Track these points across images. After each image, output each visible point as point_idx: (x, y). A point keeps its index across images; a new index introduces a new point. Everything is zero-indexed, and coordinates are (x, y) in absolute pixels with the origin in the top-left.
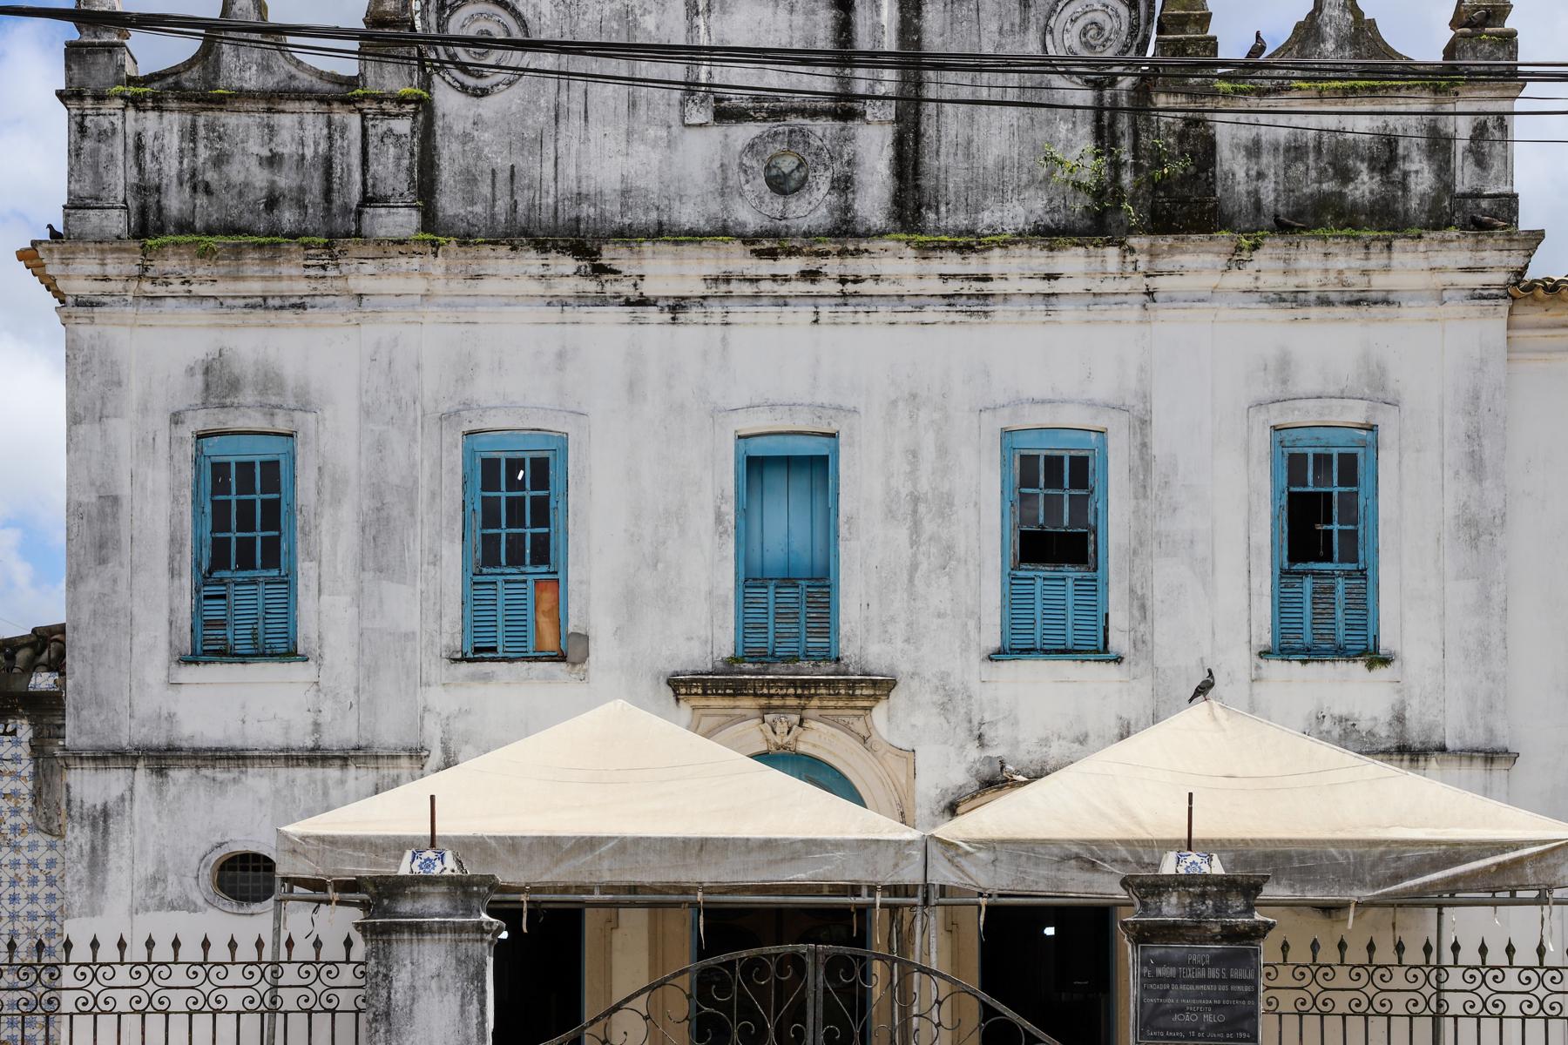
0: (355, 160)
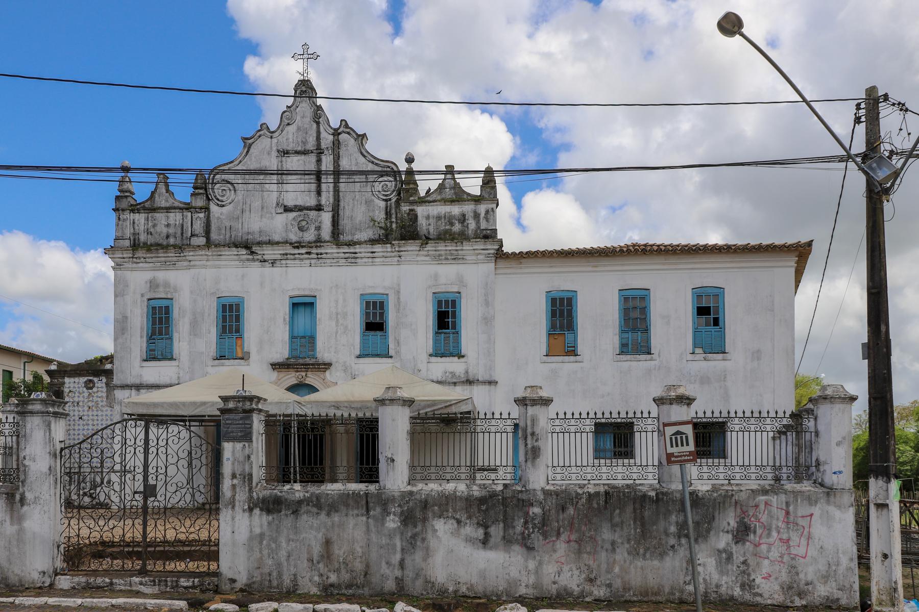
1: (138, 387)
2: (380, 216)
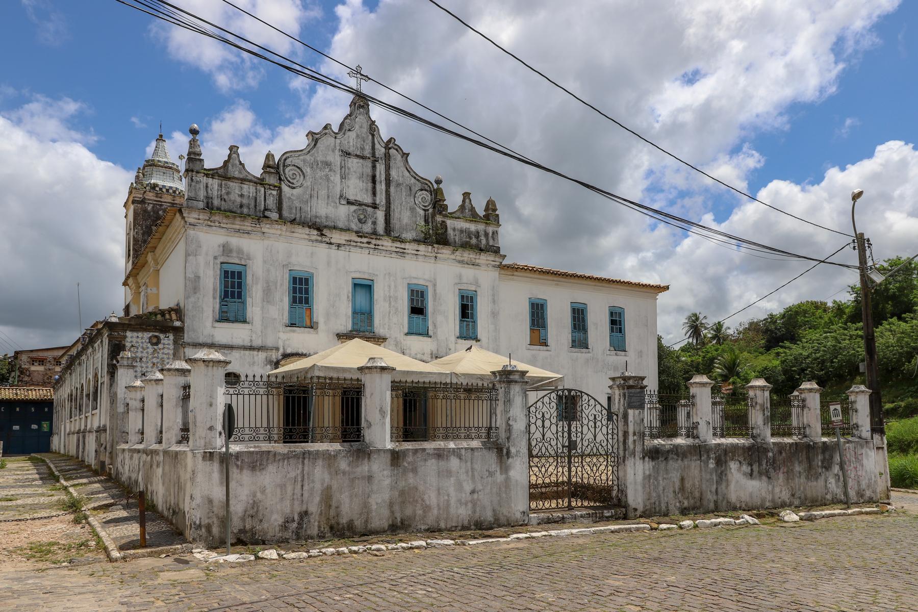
0: (263, 199)
1: (211, 346)
2: (423, 223)
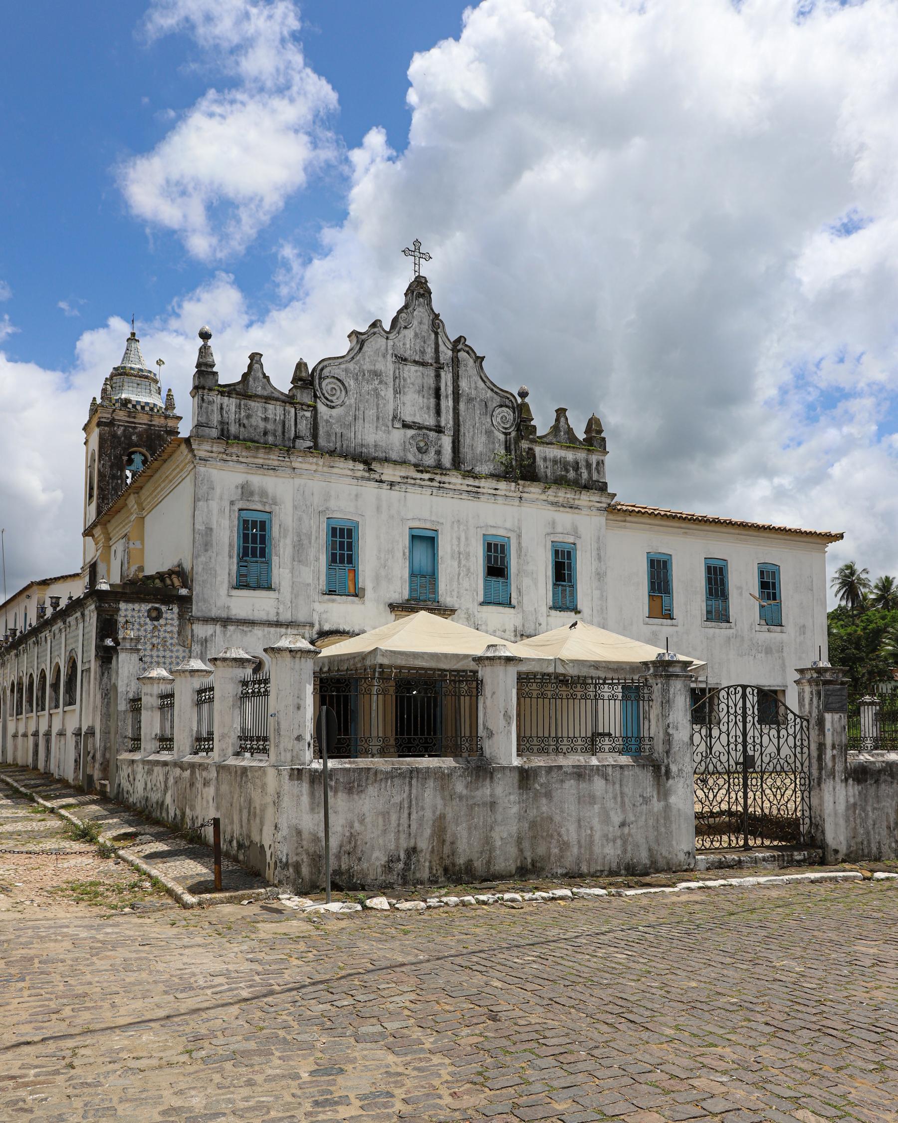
2: (503, 452)
